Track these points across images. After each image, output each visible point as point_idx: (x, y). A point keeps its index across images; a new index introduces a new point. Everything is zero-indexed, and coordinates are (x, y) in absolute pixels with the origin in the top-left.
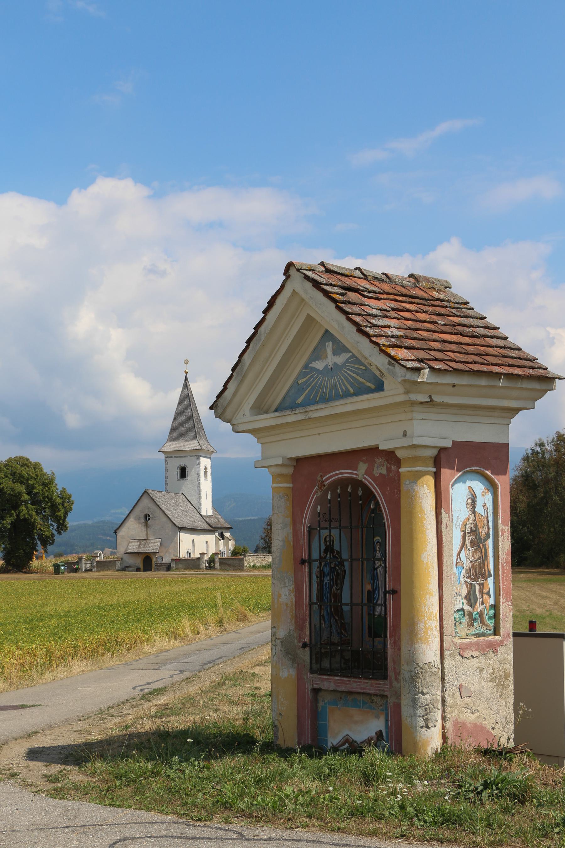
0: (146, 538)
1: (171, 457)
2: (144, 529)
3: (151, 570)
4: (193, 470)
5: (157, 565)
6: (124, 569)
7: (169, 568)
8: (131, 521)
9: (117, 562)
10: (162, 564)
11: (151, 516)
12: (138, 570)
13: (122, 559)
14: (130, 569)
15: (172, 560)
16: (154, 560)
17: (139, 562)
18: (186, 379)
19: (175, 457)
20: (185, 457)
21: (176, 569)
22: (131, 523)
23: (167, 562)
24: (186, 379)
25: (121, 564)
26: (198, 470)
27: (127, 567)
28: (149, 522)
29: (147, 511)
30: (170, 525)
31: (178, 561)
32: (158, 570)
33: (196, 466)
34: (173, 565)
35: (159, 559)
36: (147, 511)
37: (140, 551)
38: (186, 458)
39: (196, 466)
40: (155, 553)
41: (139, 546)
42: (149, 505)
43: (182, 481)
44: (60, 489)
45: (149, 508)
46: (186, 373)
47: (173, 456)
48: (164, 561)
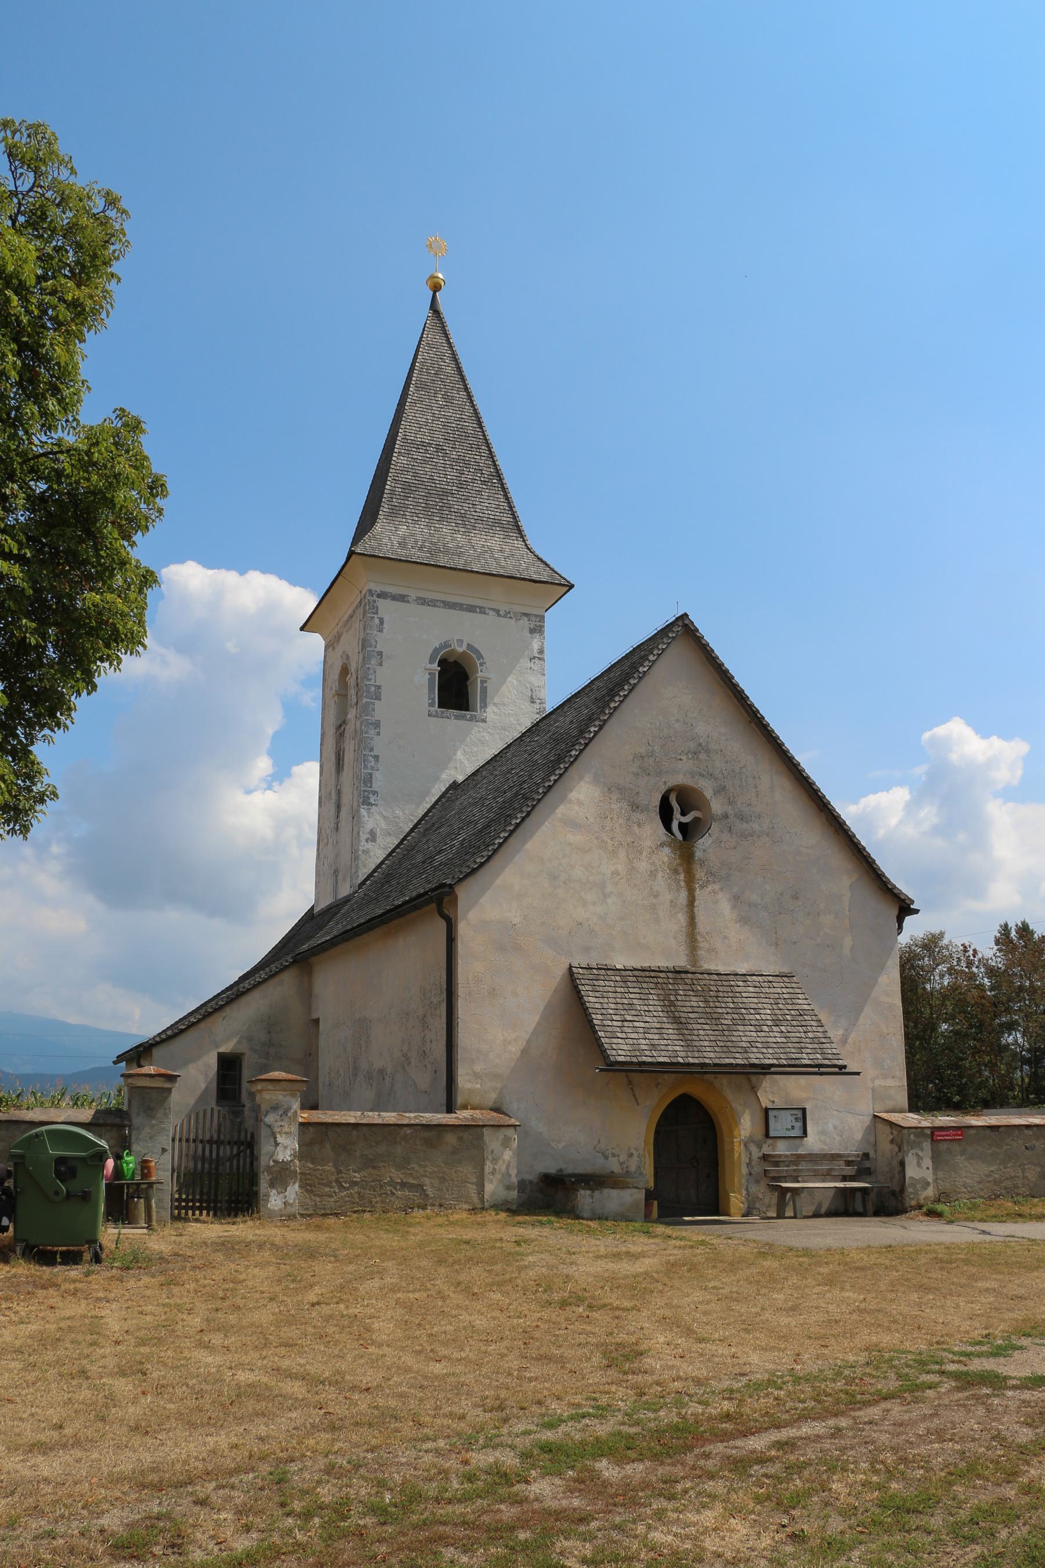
0: (681, 961)
1: (402, 598)
2: (668, 893)
4: (512, 680)
8: (573, 824)
9: (492, 1141)
11: (717, 806)
14: (614, 1199)
16: (746, 1125)
18: (434, 307)
19: (423, 601)
20: (471, 609)
22: (576, 838)
24: (434, 307)
26: (535, 680)
27: (596, 1181)
28: (704, 845)
29: (686, 764)
30: (843, 882)
33: (525, 663)
36: (686, 764)
38: (477, 617)
39: (525, 663)
40: (754, 1073)
42: (702, 729)
43: (451, 722)
44: (93, 411)
45: (700, 750)
46: (436, 288)
47: (413, 594)
48: (813, 1143)
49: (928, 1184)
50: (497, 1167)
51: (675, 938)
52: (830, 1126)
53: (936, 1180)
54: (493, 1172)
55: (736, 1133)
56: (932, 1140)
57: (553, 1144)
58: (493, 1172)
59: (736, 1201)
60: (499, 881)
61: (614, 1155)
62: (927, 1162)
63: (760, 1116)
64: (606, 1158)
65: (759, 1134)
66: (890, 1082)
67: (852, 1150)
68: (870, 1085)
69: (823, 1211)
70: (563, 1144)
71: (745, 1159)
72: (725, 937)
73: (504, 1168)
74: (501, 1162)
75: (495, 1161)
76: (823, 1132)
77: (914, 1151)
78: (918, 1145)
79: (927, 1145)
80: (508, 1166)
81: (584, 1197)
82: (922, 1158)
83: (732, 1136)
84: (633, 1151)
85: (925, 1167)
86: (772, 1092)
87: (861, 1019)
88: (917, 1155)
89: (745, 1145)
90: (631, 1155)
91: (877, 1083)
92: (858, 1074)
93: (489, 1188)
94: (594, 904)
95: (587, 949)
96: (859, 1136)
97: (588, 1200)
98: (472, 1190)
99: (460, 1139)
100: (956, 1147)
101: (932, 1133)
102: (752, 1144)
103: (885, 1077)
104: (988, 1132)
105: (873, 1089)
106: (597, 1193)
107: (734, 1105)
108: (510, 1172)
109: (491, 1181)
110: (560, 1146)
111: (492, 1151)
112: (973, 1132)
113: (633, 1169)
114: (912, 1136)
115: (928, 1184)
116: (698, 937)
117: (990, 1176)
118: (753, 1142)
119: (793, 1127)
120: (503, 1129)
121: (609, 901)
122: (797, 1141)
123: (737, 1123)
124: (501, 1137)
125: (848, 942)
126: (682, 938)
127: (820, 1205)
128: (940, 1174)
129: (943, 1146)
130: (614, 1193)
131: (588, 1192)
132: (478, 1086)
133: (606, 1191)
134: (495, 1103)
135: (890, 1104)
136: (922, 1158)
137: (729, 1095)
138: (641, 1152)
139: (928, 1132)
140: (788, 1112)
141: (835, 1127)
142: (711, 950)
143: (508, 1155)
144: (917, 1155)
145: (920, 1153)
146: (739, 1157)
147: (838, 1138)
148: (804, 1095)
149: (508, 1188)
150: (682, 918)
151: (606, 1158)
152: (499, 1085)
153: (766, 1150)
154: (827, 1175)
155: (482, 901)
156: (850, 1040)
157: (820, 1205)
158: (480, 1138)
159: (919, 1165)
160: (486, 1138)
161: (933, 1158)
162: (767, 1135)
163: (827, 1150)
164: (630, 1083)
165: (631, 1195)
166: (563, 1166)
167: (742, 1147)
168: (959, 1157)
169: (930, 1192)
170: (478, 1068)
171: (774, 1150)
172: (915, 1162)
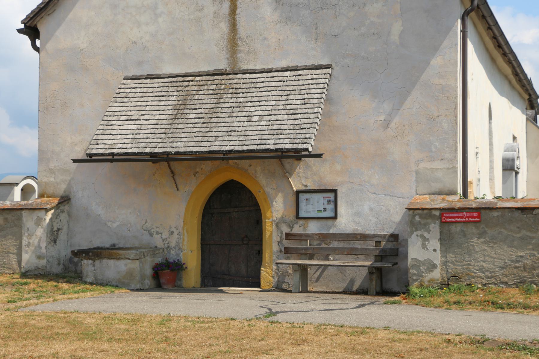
0: (223, 65)
3: (254, 282)
5: (296, 245)
6: (71, 268)
7: (386, 274)
10: (326, 244)
12: (165, 276)
13: (65, 200)
14: (112, 268)
15: (418, 216)
16: (276, 208)
17: (173, 221)
21: (453, 287)
23: (371, 227)
25: (53, 235)
27: (96, 253)
31: (461, 220)
32: (303, 282)
34: (423, 251)
35: (313, 206)
37: (181, 146)
41: (178, 113)
48: (346, 222)
49: (434, 266)
50: (31, 241)
51: (217, 45)
52: (366, 209)
53: (445, 263)
54: (28, 245)
55: (268, 214)
56: (442, 222)
57: (109, 224)
58: (28, 245)
59: (267, 275)
60: (71, 16)
61: (158, 233)
62: (435, 243)
63: (293, 199)
64: (151, 235)
65: (291, 216)
66: (437, 165)
67: (388, 230)
68: (414, 168)
69: (355, 288)
70: (117, 224)
71: (276, 238)
72: (265, 39)
73: (36, 242)
74: (34, 237)
75: (30, 236)
76: (358, 214)
77: (419, 233)
78: (425, 227)
79: (435, 227)
80: (40, 240)
81: (87, 265)
82: (428, 240)
83: (267, 218)
84: (174, 230)
85: (431, 249)
86: (300, 178)
87: (408, 103)
88: (422, 236)
89: (277, 225)
90: (172, 233)
91: (422, 165)
92: (320, 156)
93: (25, 257)
94: (147, 24)
95: (140, 63)
96: (397, 218)
97: (91, 268)
98: (13, 259)
99: (6, 219)
100: (471, 229)
101: (442, 215)
102: (283, 225)
103: (432, 159)
104: (517, 214)
105: (417, 173)
106: (97, 262)
107: (267, 189)
108: (41, 245)
109: (27, 252)
110: (115, 225)
111: (28, 229)
112: (496, 214)
113: (173, 244)
114: (417, 218)
115: (434, 266)
116: (240, 43)
117: (518, 261)
118: (285, 222)
119: (325, 210)
120: (37, 212)
121: (160, 20)
122: (330, 222)
123: (270, 206)
124: (35, 218)
125: (397, 28)
126: (224, 43)
127: (352, 282)
128: (451, 256)
129: (456, 229)
130: (111, 262)
131: (90, 262)
132: (52, 179)
133: (105, 261)
134: (65, 192)
135: (436, 187)
136: (428, 240)
137: (262, 180)
138: (181, 230)
139: (437, 213)
140: (320, 196)
141: (371, 210)
142: (251, 52)
143: (40, 232)
144: (422, 236)
145: (426, 235)
146: (271, 234)
147: (374, 220)
148: (339, 179)
149: (39, 257)
150: (224, 27)
151: (151, 235)
152: (68, 178)
153: (297, 229)
154: (351, 252)
155: (57, 33)
156: (392, 125)
157: (352, 282)
158: (20, 219)
159: (424, 247)
160: (24, 219)
161: (441, 240)
162: (298, 217)
163: (360, 230)
164: (172, 172)
165: (126, 265)
166: (116, 242)
167: (274, 226)
168: (475, 240)
169: (437, 274)
170: (52, 165)
171: (305, 228)
172: (419, 243)
